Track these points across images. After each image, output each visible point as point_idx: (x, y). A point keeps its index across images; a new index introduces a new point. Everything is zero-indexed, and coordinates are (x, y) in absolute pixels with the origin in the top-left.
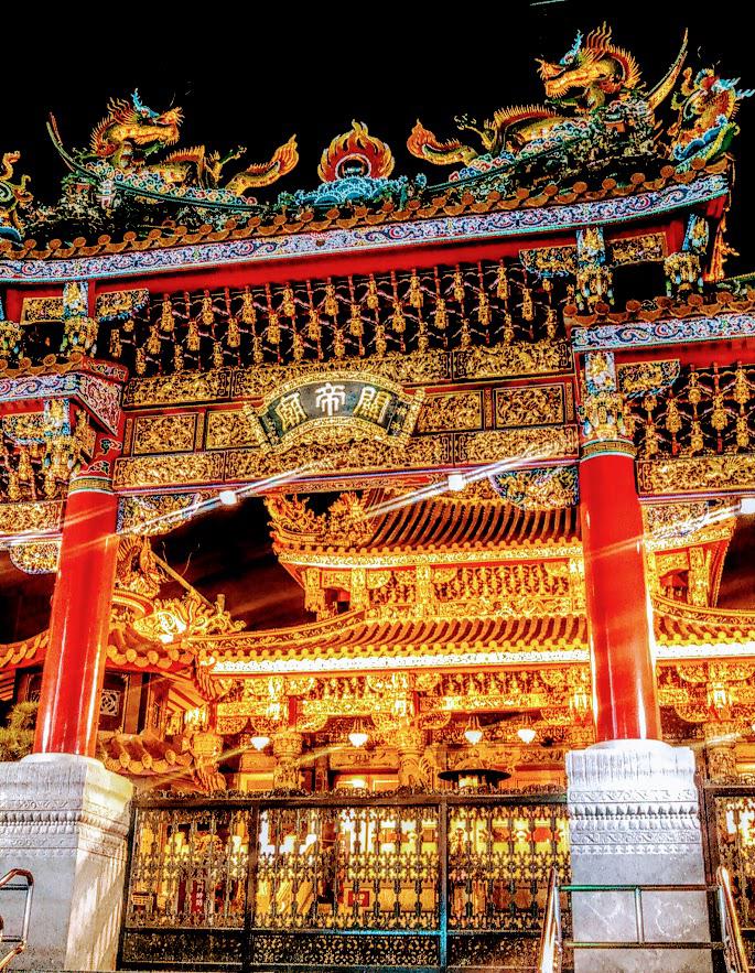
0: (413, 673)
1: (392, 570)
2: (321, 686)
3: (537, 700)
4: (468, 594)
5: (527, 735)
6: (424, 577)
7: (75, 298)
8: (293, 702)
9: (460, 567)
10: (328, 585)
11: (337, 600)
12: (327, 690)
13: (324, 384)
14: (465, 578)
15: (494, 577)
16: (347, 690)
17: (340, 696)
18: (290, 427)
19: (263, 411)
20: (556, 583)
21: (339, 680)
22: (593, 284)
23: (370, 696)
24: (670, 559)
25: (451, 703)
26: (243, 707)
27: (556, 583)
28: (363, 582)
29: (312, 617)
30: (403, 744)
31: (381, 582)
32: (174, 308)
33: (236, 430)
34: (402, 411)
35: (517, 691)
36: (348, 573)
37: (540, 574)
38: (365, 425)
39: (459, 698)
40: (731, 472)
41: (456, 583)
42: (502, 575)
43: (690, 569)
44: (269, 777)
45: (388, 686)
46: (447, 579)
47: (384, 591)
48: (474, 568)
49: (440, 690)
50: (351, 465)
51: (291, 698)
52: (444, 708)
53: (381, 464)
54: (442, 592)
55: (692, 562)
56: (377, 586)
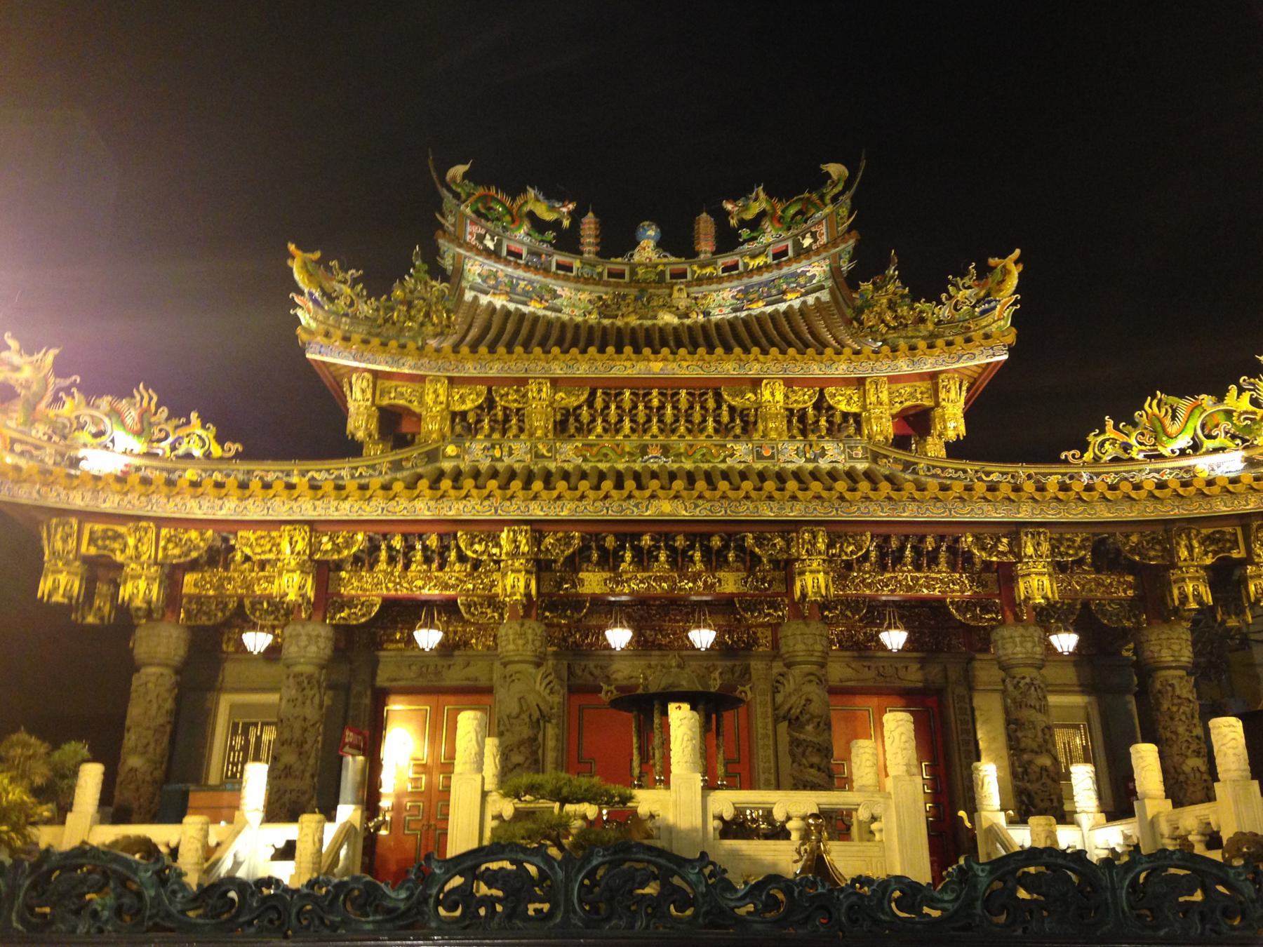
0: (538, 529)
1: (489, 382)
2: (373, 548)
3: (731, 582)
4: (599, 430)
5: (703, 637)
6: (540, 403)
8: (324, 572)
9: (593, 386)
10: (385, 402)
11: (395, 426)
12: (383, 555)
14: (599, 404)
15: (641, 407)
16: (419, 556)
17: (407, 567)
21: (405, 537)
23: (457, 567)
24: (906, 389)
26: (230, 579)
27: (732, 420)
28: (442, 398)
29: (353, 449)
30: (511, 647)
31: (470, 401)
35: (699, 566)
36: (417, 386)
37: (711, 404)
39: (606, 575)
41: (585, 411)
42: (655, 403)
43: (938, 404)
44: (273, 698)
45: (495, 551)
46: (573, 402)
47: (471, 419)
48: (613, 388)
49: (575, 563)
51: (320, 563)
52: (580, 590)
54: (565, 424)
55: (942, 395)
56: (464, 407)
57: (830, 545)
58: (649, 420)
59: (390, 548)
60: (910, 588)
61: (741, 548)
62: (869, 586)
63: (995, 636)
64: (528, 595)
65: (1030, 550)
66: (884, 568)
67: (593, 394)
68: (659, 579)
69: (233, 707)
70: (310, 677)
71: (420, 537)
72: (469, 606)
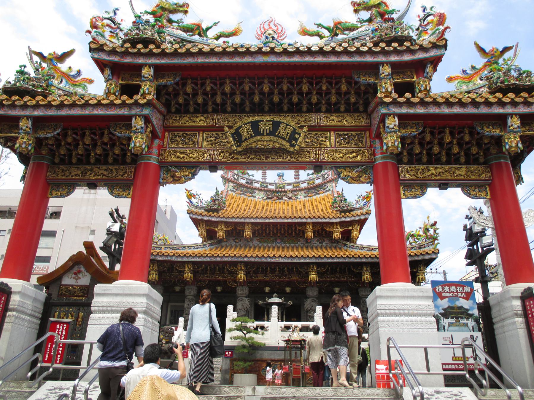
7: (147, 72)
13: (263, 121)
18: (246, 139)
19: (233, 131)
20: (299, 232)
22: (386, 87)
25: (260, 278)
27: (299, 232)
32: (192, 83)
33: (217, 140)
34: (297, 136)
35: (287, 273)
38: (280, 141)
40: (438, 173)
42: (279, 228)
50: (272, 159)
53: (285, 159)
57: (317, 268)
58: (277, 232)
59: (210, 267)
60: (339, 278)
61: (297, 268)
62: (328, 278)
63: (359, 290)
64: (244, 280)
65: (365, 269)
66: (333, 274)
67: (262, 225)
68: (276, 276)
69: (171, 306)
70: (192, 299)
71: (218, 265)
72: (229, 283)
